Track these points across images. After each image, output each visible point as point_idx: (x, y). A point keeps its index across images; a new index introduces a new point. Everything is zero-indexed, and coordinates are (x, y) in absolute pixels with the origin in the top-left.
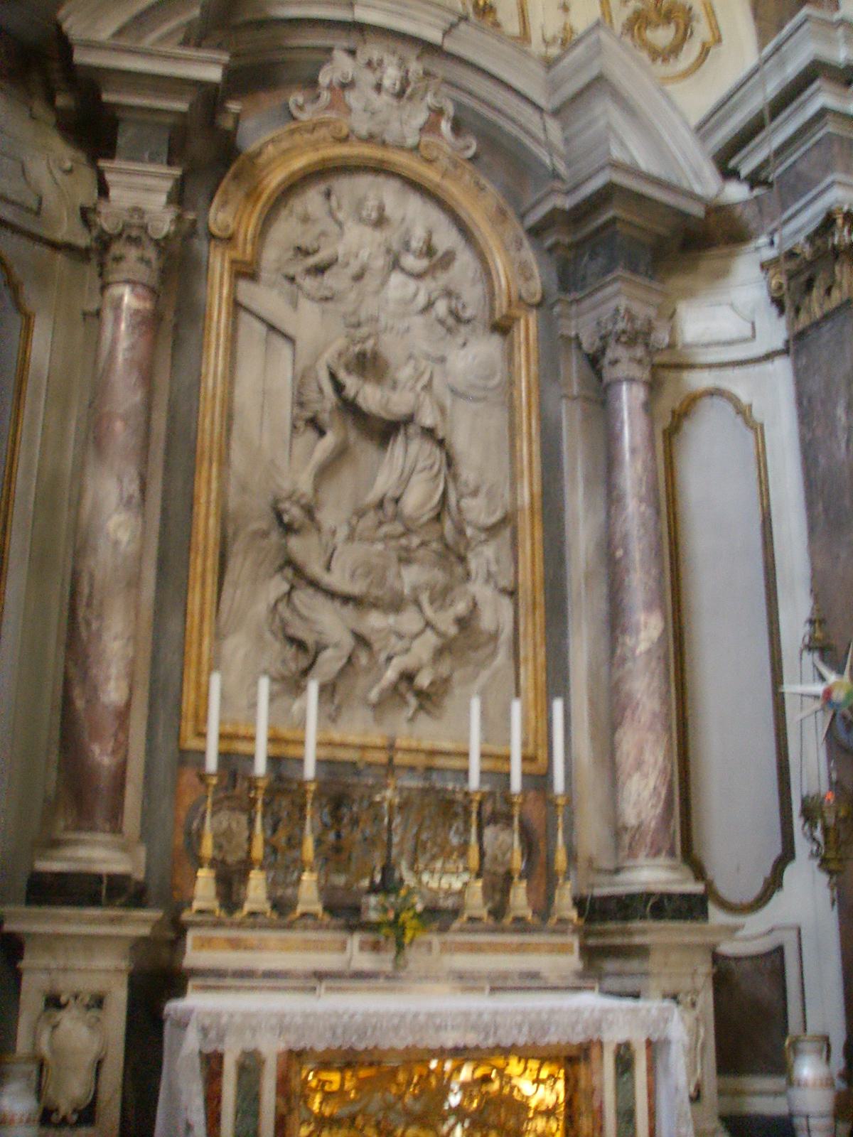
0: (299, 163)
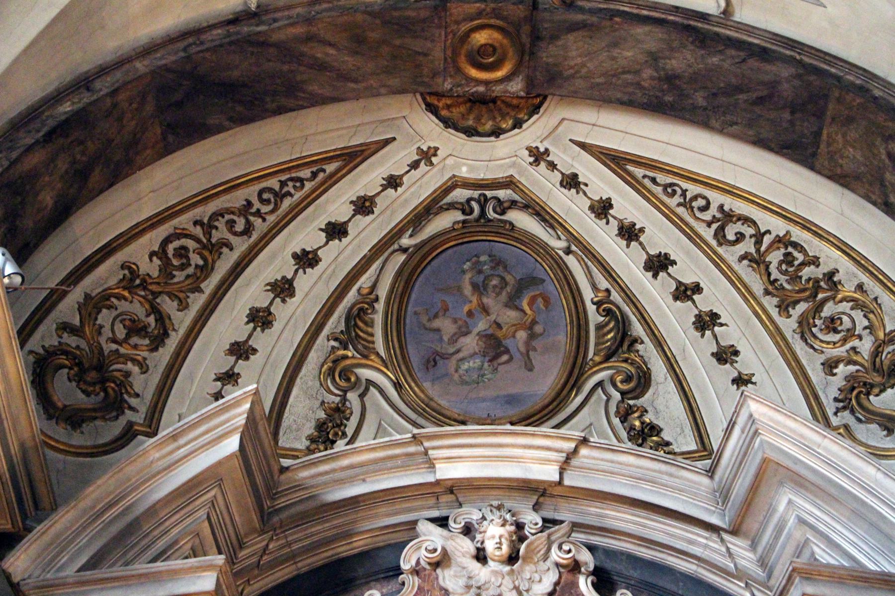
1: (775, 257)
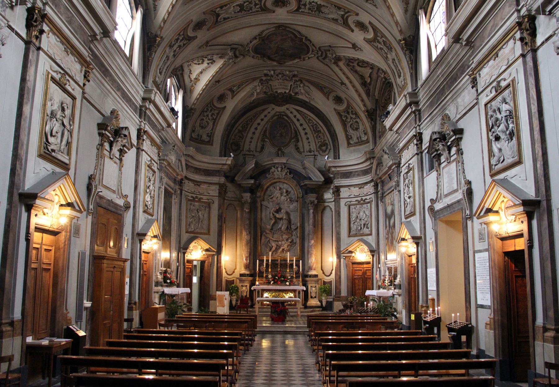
1: (315, 126)
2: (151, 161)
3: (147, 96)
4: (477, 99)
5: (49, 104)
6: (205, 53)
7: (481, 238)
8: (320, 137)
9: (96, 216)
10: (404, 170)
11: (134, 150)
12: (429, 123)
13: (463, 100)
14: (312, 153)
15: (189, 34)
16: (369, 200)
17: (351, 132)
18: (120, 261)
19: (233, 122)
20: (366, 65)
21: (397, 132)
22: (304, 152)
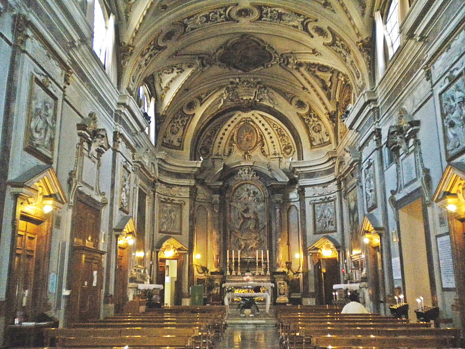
0: (236, 186)
1: (279, 130)
2: (126, 162)
3: (122, 101)
4: (432, 90)
5: (33, 102)
6: (175, 63)
7: (442, 222)
8: (284, 140)
9: (76, 208)
10: (365, 166)
11: (110, 151)
12: (388, 119)
13: (419, 93)
14: (277, 156)
15: (159, 44)
16: (333, 198)
17: (313, 134)
18: (99, 253)
19: (201, 128)
20: (326, 69)
21: (357, 130)
22: (269, 155)
